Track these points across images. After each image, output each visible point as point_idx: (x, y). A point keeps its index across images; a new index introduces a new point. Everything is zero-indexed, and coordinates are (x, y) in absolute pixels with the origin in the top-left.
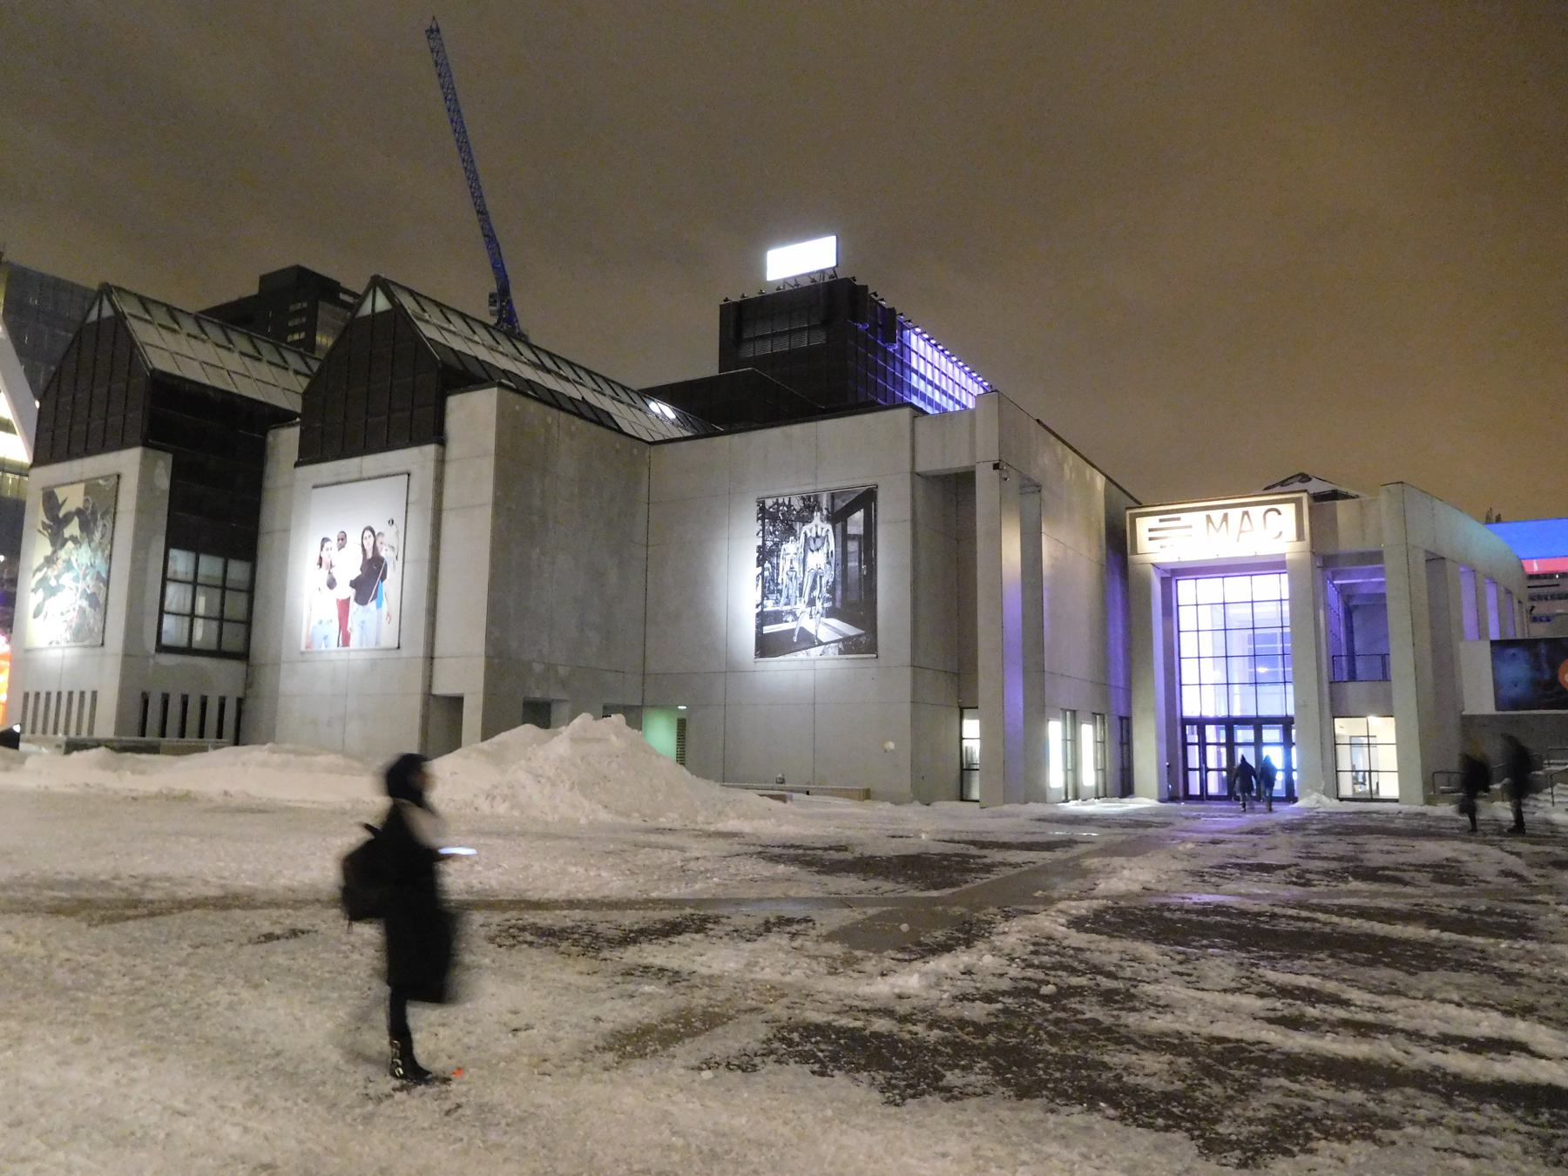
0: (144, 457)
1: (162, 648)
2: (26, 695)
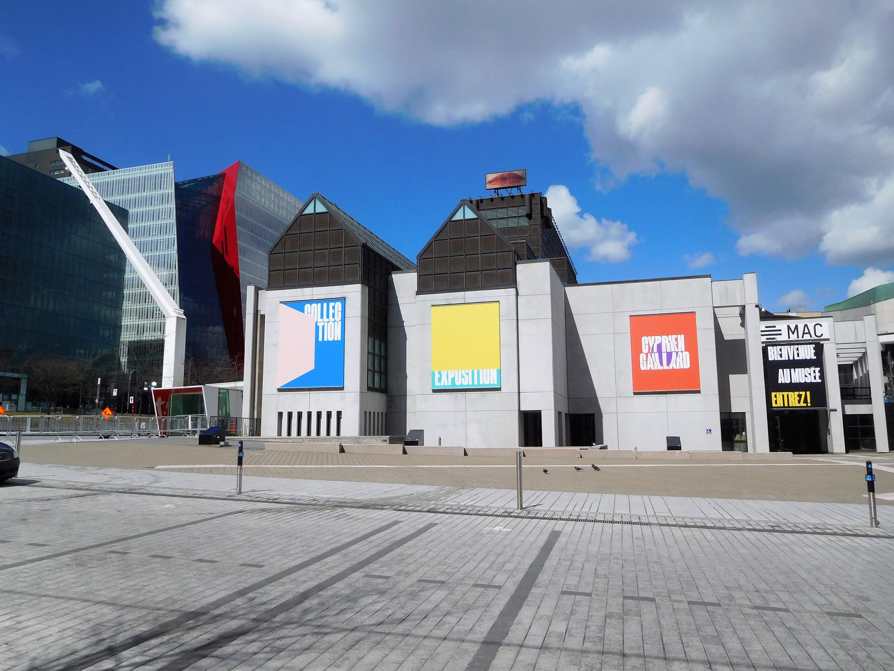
1: (370, 389)
2: (280, 415)
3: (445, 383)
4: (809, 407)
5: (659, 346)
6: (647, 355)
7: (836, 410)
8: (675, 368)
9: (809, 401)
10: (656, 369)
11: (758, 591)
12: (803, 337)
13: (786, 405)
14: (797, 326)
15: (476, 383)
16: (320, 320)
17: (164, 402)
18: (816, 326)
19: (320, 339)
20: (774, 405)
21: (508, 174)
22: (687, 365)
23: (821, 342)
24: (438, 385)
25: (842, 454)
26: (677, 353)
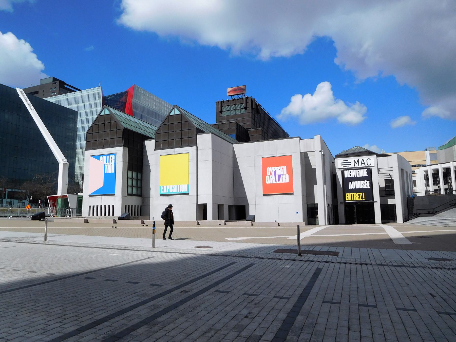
0: (123, 148)
1: (128, 195)
2: (90, 207)
3: (166, 192)
4: (364, 200)
5: (275, 172)
6: (269, 176)
7: (377, 202)
8: (282, 182)
9: (364, 198)
10: (273, 183)
12: (361, 166)
13: (353, 200)
14: (358, 160)
15: (178, 191)
16: (106, 164)
17: (54, 202)
18: (368, 160)
19: (106, 173)
20: (347, 200)
21: (237, 88)
22: (287, 181)
23: (370, 168)
24: (163, 192)
25: (380, 224)
26: (283, 175)
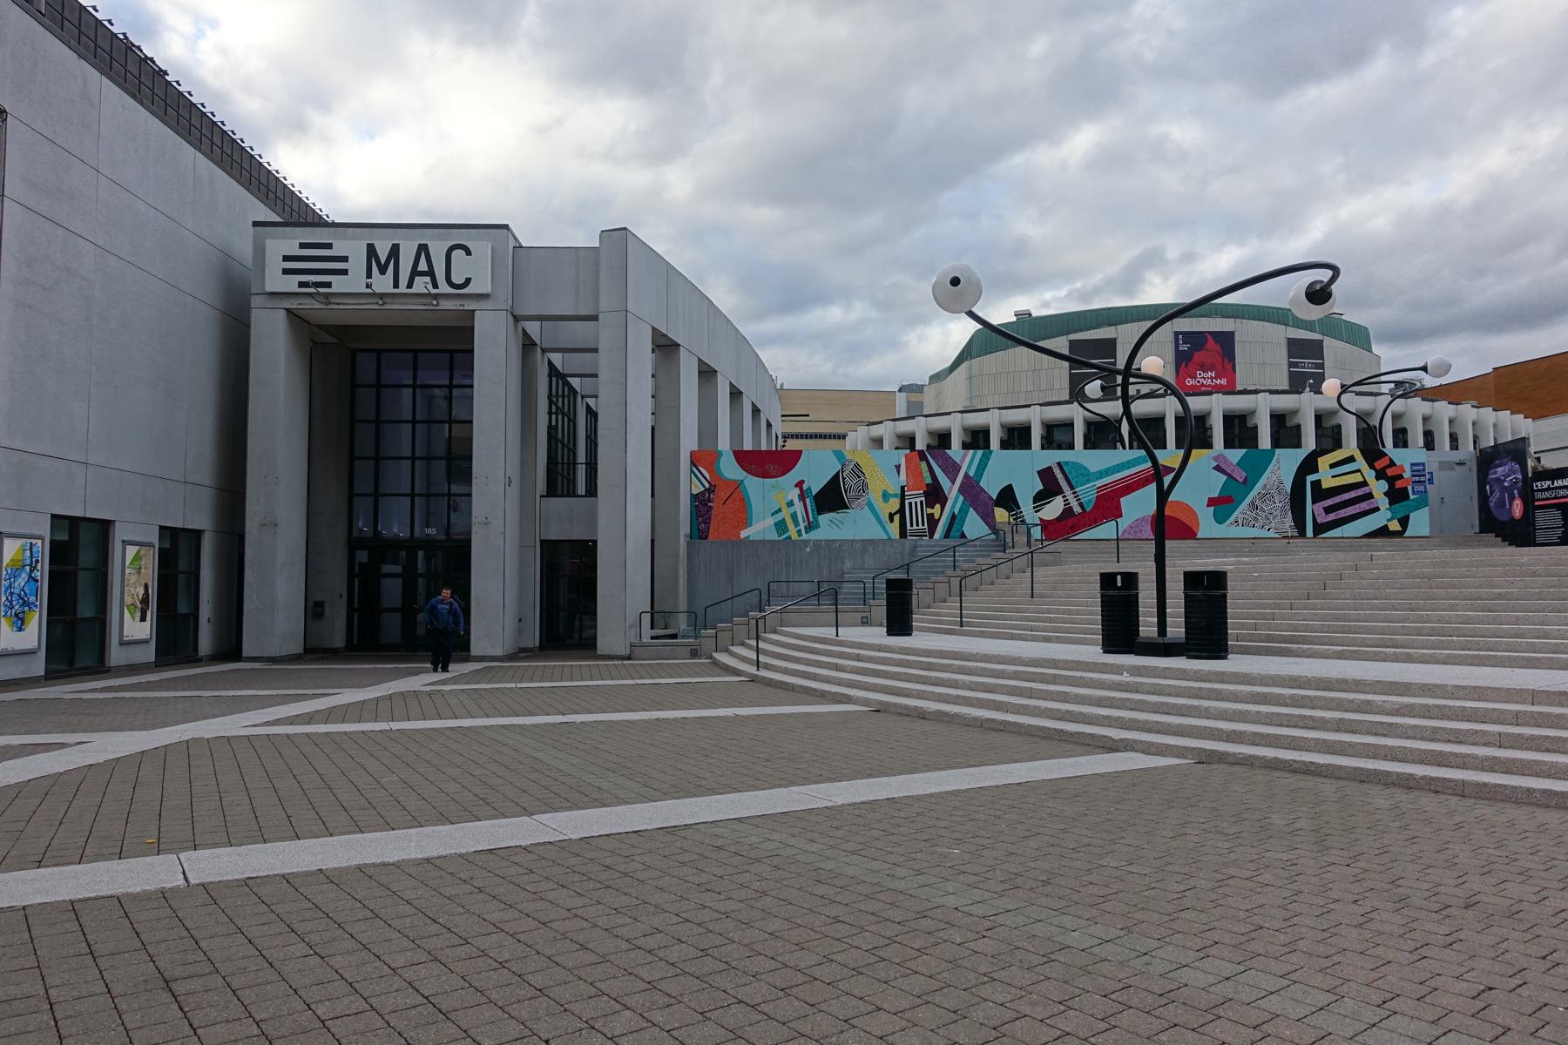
11: (649, 952)
12: (410, 285)
18: (455, 253)
